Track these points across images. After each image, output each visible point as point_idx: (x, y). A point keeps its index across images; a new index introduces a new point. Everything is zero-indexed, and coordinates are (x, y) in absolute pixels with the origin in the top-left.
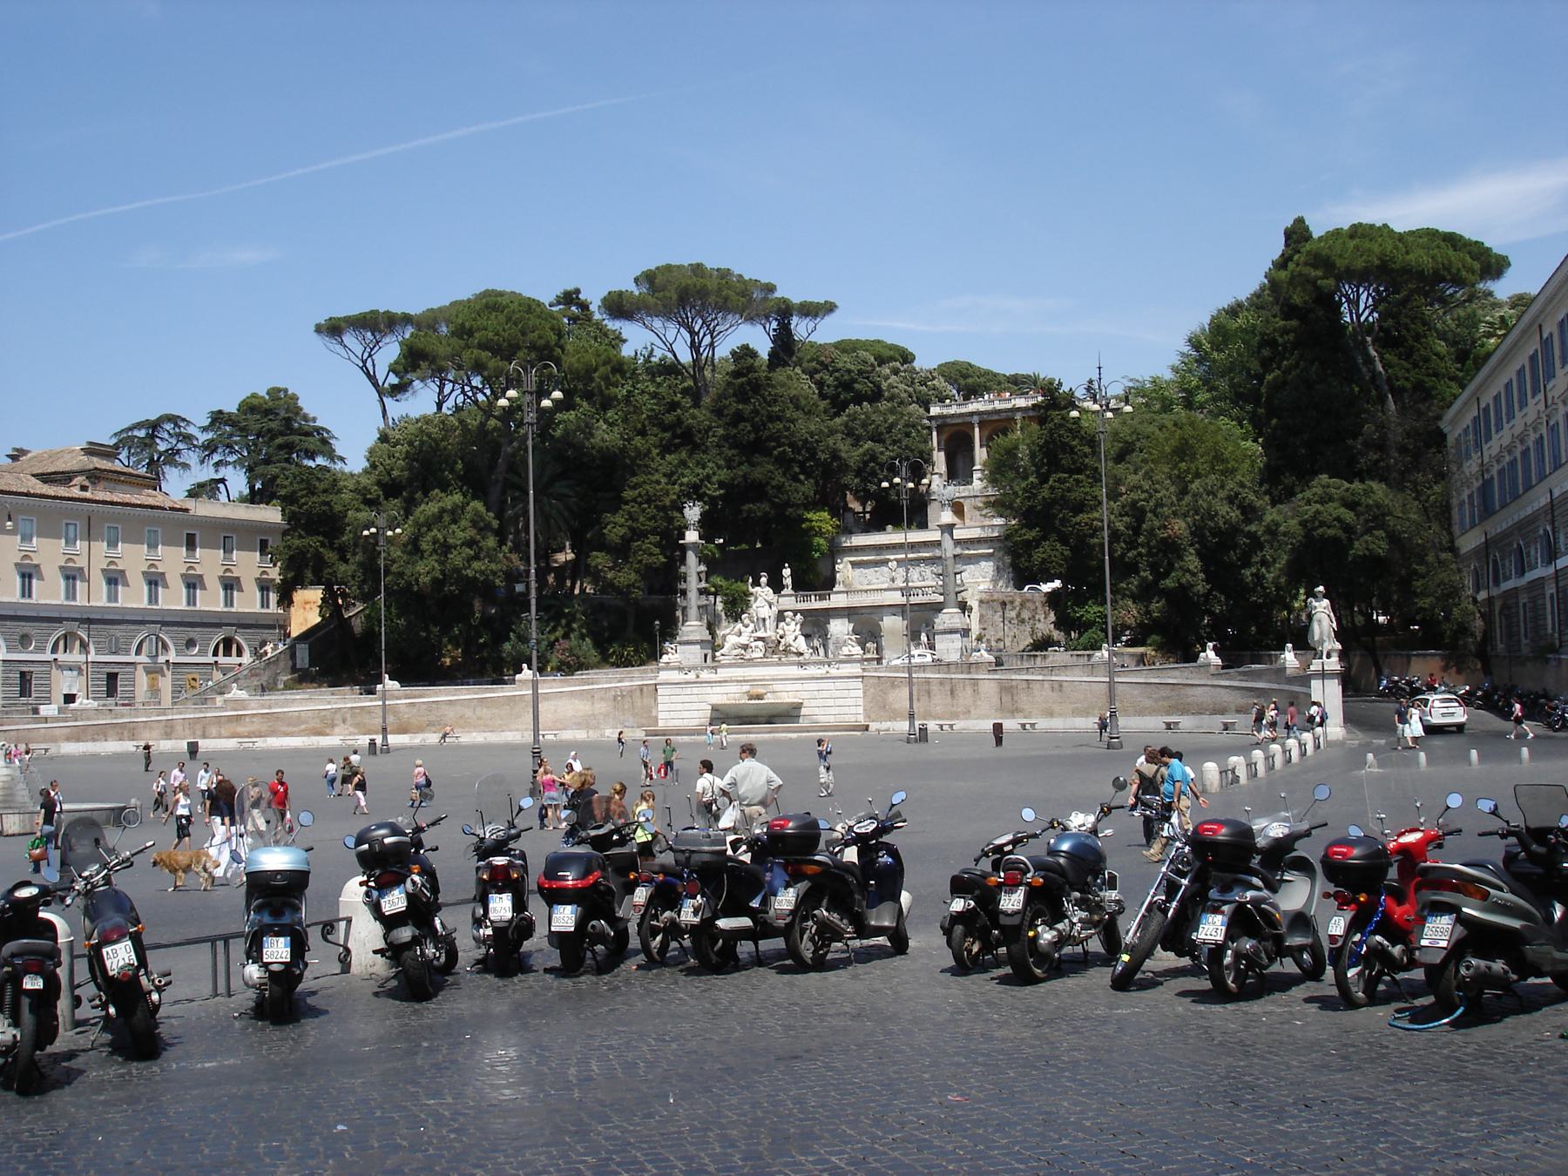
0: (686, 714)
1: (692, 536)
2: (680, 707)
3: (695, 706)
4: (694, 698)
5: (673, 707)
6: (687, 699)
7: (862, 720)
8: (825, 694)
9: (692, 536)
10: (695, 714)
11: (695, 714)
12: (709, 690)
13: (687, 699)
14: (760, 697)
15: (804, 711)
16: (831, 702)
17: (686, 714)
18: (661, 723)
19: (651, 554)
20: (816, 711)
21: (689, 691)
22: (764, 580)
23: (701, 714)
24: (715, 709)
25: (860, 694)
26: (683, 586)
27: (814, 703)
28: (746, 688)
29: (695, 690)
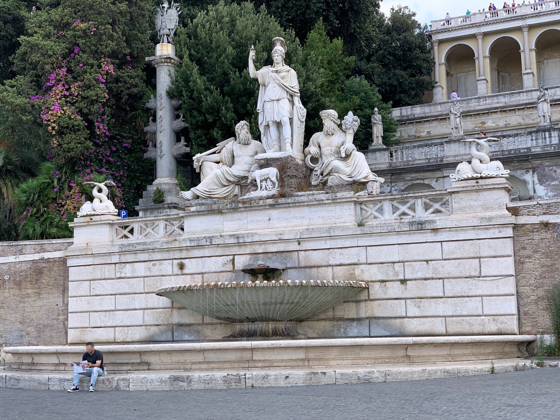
1: (165, 49)
2: (108, 303)
3: (140, 301)
4: (138, 285)
5: (96, 304)
8: (422, 271)
10: (137, 317)
14: (269, 273)
17: (121, 318)
18: (72, 336)
20: (399, 309)
21: (128, 270)
22: (279, 51)
23: (150, 318)
25: (508, 266)
27: (395, 289)
28: (241, 262)
29: (141, 269)
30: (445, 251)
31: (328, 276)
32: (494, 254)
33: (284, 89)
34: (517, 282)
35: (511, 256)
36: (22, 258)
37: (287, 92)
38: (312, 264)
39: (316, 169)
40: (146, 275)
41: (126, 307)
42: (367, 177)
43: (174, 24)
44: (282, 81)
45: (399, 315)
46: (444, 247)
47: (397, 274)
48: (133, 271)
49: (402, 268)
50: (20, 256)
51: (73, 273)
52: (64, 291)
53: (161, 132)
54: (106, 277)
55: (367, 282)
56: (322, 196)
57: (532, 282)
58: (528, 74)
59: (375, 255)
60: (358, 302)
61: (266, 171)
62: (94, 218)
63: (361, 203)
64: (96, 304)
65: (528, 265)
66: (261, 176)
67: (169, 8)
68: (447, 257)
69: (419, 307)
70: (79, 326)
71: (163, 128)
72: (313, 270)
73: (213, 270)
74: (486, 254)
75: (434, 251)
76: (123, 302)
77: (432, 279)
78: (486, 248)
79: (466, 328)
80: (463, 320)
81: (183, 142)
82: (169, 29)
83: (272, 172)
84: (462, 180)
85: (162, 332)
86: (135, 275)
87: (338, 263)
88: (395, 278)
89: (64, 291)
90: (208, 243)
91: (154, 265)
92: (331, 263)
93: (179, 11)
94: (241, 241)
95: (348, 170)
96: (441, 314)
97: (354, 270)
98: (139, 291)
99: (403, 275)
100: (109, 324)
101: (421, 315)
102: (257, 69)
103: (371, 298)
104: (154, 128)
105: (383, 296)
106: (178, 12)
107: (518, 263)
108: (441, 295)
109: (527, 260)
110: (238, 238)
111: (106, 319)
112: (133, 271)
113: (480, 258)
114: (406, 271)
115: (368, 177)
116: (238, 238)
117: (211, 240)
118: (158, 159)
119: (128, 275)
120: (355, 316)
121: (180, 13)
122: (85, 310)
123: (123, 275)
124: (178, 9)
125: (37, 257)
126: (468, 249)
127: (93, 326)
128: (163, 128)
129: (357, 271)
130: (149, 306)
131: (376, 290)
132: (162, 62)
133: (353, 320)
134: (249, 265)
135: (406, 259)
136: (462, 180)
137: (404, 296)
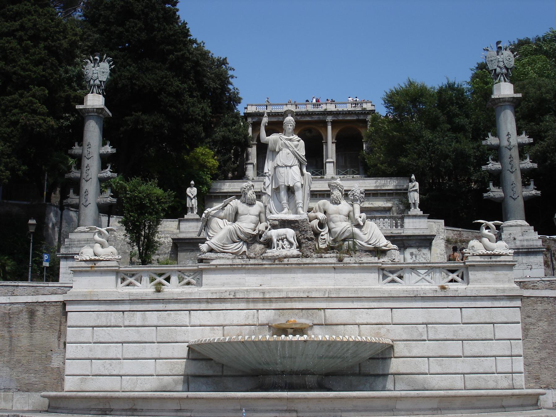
0: (129, 367)
2: (114, 351)
3: (150, 350)
4: (149, 334)
5: (99, 351)
6: (132, 334)
7: (522, 385)
8: (442, 332)
9: (95, 100)
10: (149, 367)
11: (149, 367)
12: (183, 317)
13: (132, 334)
15: (395, 365)
16: (455, 348)
17: (129, 367)
19: (34, 112)
20: (423, 365)
23: (162, 367)
24: (196, 353)
25: (516, 331)
26: (74, 174)
27: (418, 349)
29: (153, 318)
30: (464, 317)
31: (351, 335)
32: (505, 320)
33: (297, 157)
34: (524, 344)
35: (518, 323)
36: (13, 299)
37: (298, 160)
38: (339, 322)
39: (322, 233)
40: (159, 324)
41: (136, 356)
42: (387, 245)
43: (106, 76)
44: (296, 150)
45: (422, 371)
46: (463, 313)
47: (421, 334)
48: (144, 319)
49: (426, 329)
50: (11, 297)
51: (72, 319)
52: (59, 337)
53: (87, 181)
54: (112, 324)
55: (393, 341)
56: (331, 258)
57: (536, 345)
58: (330, 162)
59: (399, 316)
60: (386, 359)
61: (282, 231)
62: (99, 264)
63: (383, 269)
64: (99, 351)
65: (531, 332)
66: (278, 236)
67: (101, 61)
68: (466, 321)
69: (441, 365)
70: (78, 373)
71: (89, 177)
72: (339, 326)
73: (235, 322)
74: (499, 320)
75: (454, 315)
76: (131, 350)
77: (453, 340)
78: (499, 315)
79: (483, 385)
80: (480, 377)
81: (108, 192)
82: (101, 81)
83: (290, 233)
84: (477, 255)
85: (176, 382)
86: (146, 324)
87: (365, 322)
88: (419, 338)
89: (59, 337)
90: (232, 297)
91: (168, 315)
92: (357, 322)
93: (113, 65)
94: (267, 296)
95: (366, 238)
96: (460, 371)
97: (379, 329)
98: (151, 340)
99: (426, 335)
100: (114, 373)
101: (442, 372)
102: (268, 135)
103: (396, 355)
104: (78, 175)
105: (408, 355)
106: (110, 66)
107: (525, 330)
108: (461, 354)
109: (532, 327)
110: (264, 293)
111: (111, 368)
112: (144, 319)
113: (493, 323)
114: (429, 332)
115: (388, 246)
116: (264, 293)
117: (235, 293)
118: (82, 207)
119: (138, 324)
120: (381, 373)
121: (112, 67)
122: (87, 356)
123: (132, 323)
124: (111, 63)
125: (30, 299)
126: (483, 315)
127: (96, 373)
128: (89, 177)
129: (383, 330)
130: (162, 356)
131: (400, 349)
132: (93, 112)
133: (378, 376)
134: (275, 320)
135: (430, 321)
136: (477, 255)
137: (427, 355)
